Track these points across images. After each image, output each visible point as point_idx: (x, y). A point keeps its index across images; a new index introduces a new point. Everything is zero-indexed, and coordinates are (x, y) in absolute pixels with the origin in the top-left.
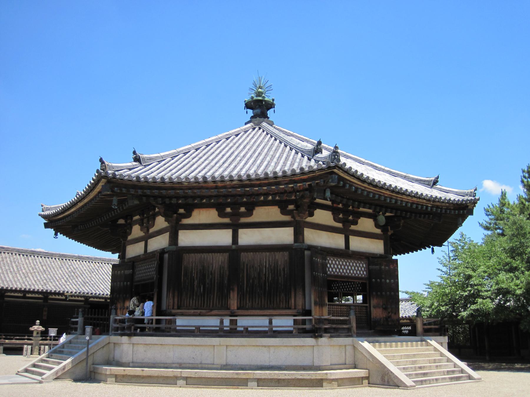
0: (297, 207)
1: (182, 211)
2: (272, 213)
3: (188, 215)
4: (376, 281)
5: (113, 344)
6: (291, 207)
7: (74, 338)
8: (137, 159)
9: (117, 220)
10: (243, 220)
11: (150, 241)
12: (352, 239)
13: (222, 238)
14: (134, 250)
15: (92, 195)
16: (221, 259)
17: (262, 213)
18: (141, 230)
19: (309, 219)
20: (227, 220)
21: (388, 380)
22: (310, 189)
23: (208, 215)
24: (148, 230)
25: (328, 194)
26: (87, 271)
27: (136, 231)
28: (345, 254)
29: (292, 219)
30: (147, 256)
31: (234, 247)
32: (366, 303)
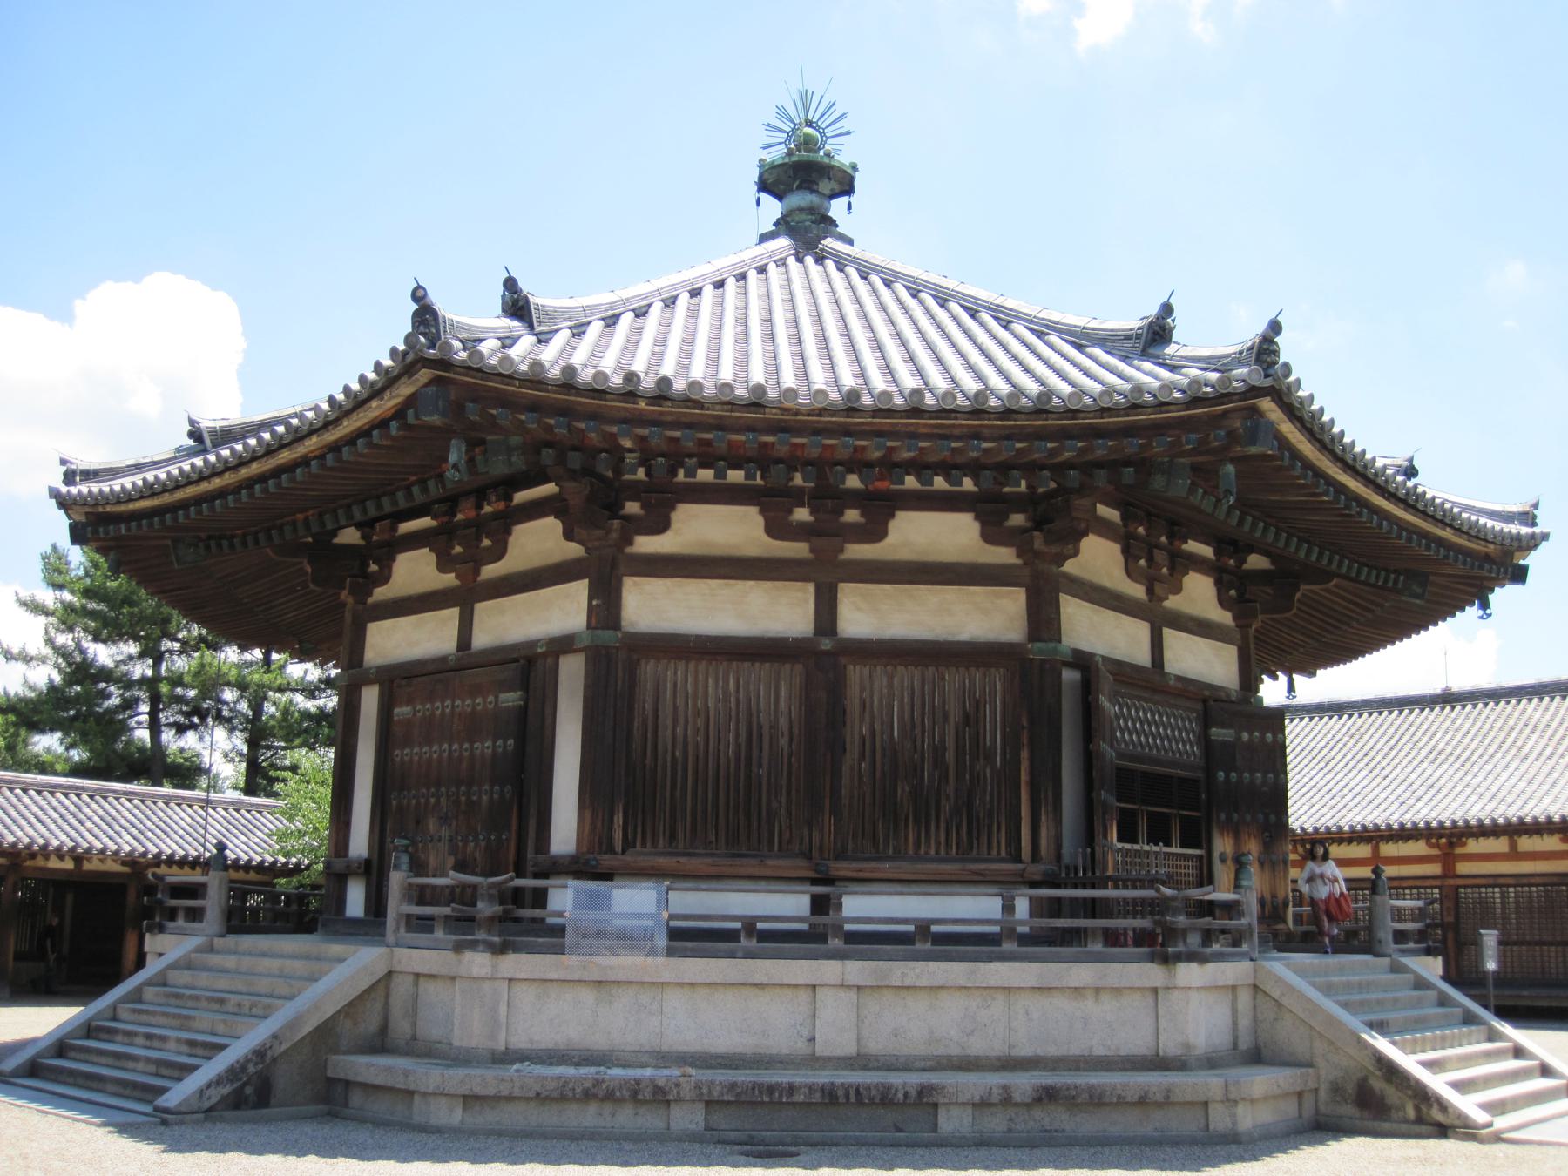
1: (632, 507)
4: (1227, 776)
5: (411, 978)
6: (1017, 519)
7: (198, 950)
8: (517, 306)
11: (482, 609)
13: (781, 611)
14: (395, 641)
18: (442, 568)
23: (729, 527)
24: (477, 572)
27: (415, 570)
28: (1150, 681)
29: (1018, 561)
31: (826, 644)
32: (1198, 847)
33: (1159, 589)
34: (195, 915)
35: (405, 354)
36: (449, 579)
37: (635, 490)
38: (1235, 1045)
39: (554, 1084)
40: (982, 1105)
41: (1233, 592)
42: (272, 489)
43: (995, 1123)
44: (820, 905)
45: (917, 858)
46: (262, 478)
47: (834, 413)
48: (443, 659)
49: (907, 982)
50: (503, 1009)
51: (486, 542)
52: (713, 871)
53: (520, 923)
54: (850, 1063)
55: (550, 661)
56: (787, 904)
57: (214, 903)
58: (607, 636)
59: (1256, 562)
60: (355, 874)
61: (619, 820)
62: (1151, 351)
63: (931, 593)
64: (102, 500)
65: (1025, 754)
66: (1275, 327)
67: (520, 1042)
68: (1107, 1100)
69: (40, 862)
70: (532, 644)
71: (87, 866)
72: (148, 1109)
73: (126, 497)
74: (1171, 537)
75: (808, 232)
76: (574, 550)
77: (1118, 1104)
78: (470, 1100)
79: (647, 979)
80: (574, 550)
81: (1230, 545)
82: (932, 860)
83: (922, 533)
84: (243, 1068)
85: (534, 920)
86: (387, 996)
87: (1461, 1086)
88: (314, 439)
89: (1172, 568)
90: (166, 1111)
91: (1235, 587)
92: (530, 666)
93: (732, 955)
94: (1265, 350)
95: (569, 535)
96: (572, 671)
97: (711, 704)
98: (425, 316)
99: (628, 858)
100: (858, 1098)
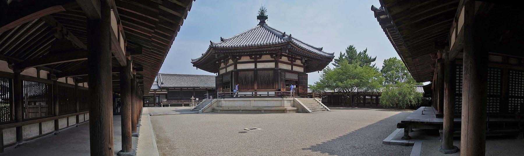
0: (276, 55)
2: (268, 57)
3: (240, 59)
6: (274, 55)
10: (258, 60)
13: (252, 66)
14: (223, 72)
16: (251, 74)
17: (264, 58)
19: (280, 60)
20: (253, 60)
21: (304, 111)
22: (281, 49)
25: (287, 51)
26: (208, 78)
27: (223, 65)
28: (292, 72)
30: (227, 73)
54: (253, 107)
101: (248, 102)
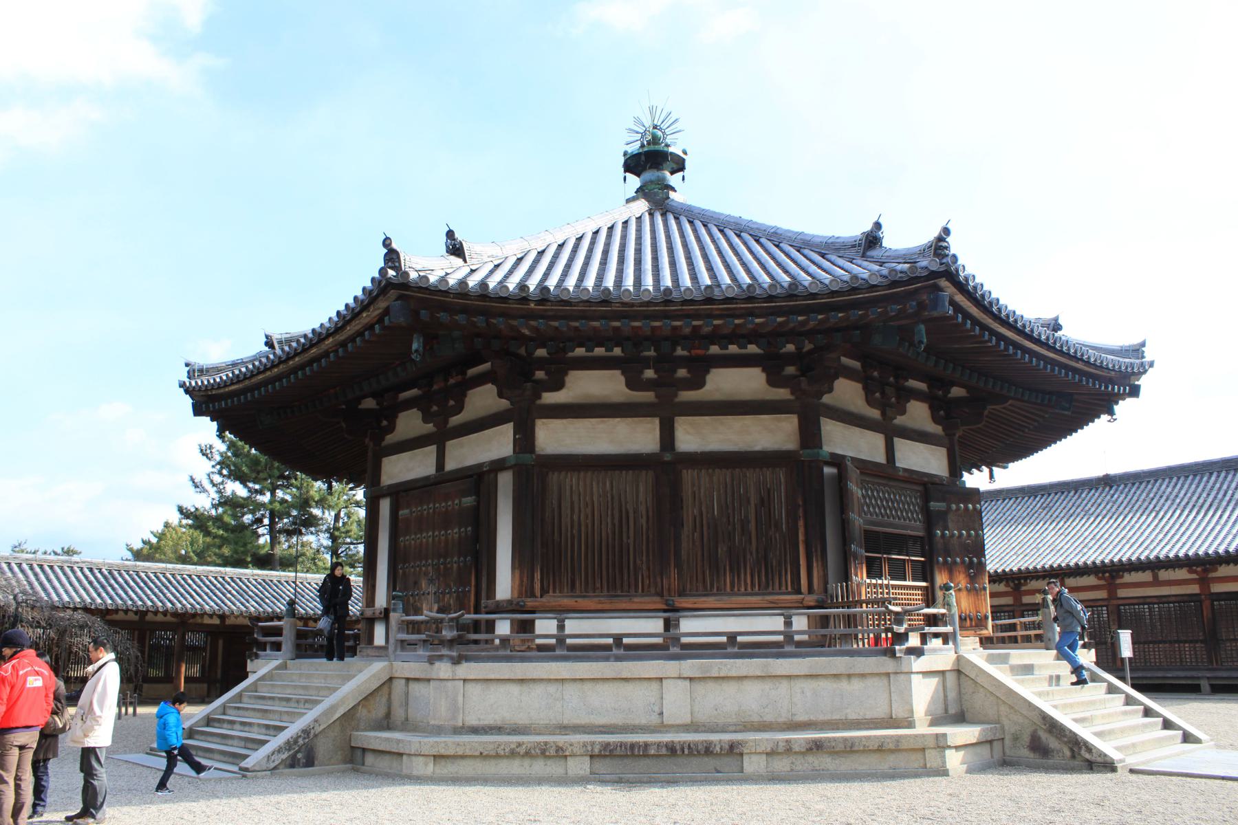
1: (540, 374)
2: (747, 382)
5: (403, 681)
6: (790, 370)
7: (277, 668)
9: (359, 400)
10: (687, 396)
12: (901, 445)
13: (638, 437)
15: (350, 330)
18: (425, 421)
20: (648, 396)
23: (603, 384)
24: (446, 422)
27: (410, 423)
28: (885, 474)
29: (792, 397)
31: (668, 457)
33: (889, 412)
34: (277, 647)
35: (380, 282)
36: (429, 427)
37: (541, 363)
38: (946, 710)
39: (492, 746)
40: (771, 754)
41: (942, 413)
42: (308, 373)
43: (781, 765)
44: (668, 625)
45: (732, 593)
46: (302, 367)
47: (656, 304)
48: (427, 478)
49: (722, 675)
50: (460, 699)
51: (452, 403)
52: (600, 607)
53: (469, 640)
54: (686, 728)
55: (492, 475)
56: (654, 625)
57: (287, 640)
58: (527, 458)
59: (957, 392)
60: (379, 619)
61: (538, 576)
62: (869, 253)
63: (734, 422)
64: (211, 387)
65: (801, 523)
66: (946, 231)
67: (472, 721)
68: (855, 748)
69: (199, 620)
70: (480, 465)
71: (228, 622)
72: (235, 769)
73: (225, 384)
74: (896, 378)
75: (657, 198)
76: (504, 404)
77: (863, 751)
78: (438, 758)
79: (552, 677)
80: (504, 404)
81: (938, 383)
82: (744, 595)
83: (729, 382)
84: (296, 742)
85: (487, 642)
86: (390, 694)
87: (1099, 734)
88: (331, 340)
89: (898, 398)
90: (246, 770)
91: (941, 408)
92: (479, 480)
93: (607, 659)
94: (939, 247)
95: (501, 395)
96: (505, 481)
97: (595, 499)
98: (392, 256)
99: (544, 600)
100: (691, 751)
101: (650, 692)
